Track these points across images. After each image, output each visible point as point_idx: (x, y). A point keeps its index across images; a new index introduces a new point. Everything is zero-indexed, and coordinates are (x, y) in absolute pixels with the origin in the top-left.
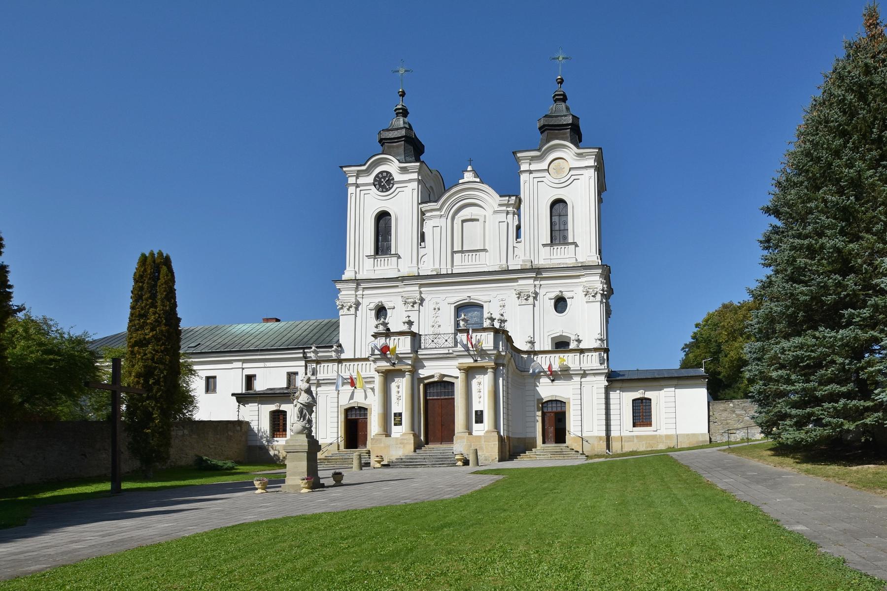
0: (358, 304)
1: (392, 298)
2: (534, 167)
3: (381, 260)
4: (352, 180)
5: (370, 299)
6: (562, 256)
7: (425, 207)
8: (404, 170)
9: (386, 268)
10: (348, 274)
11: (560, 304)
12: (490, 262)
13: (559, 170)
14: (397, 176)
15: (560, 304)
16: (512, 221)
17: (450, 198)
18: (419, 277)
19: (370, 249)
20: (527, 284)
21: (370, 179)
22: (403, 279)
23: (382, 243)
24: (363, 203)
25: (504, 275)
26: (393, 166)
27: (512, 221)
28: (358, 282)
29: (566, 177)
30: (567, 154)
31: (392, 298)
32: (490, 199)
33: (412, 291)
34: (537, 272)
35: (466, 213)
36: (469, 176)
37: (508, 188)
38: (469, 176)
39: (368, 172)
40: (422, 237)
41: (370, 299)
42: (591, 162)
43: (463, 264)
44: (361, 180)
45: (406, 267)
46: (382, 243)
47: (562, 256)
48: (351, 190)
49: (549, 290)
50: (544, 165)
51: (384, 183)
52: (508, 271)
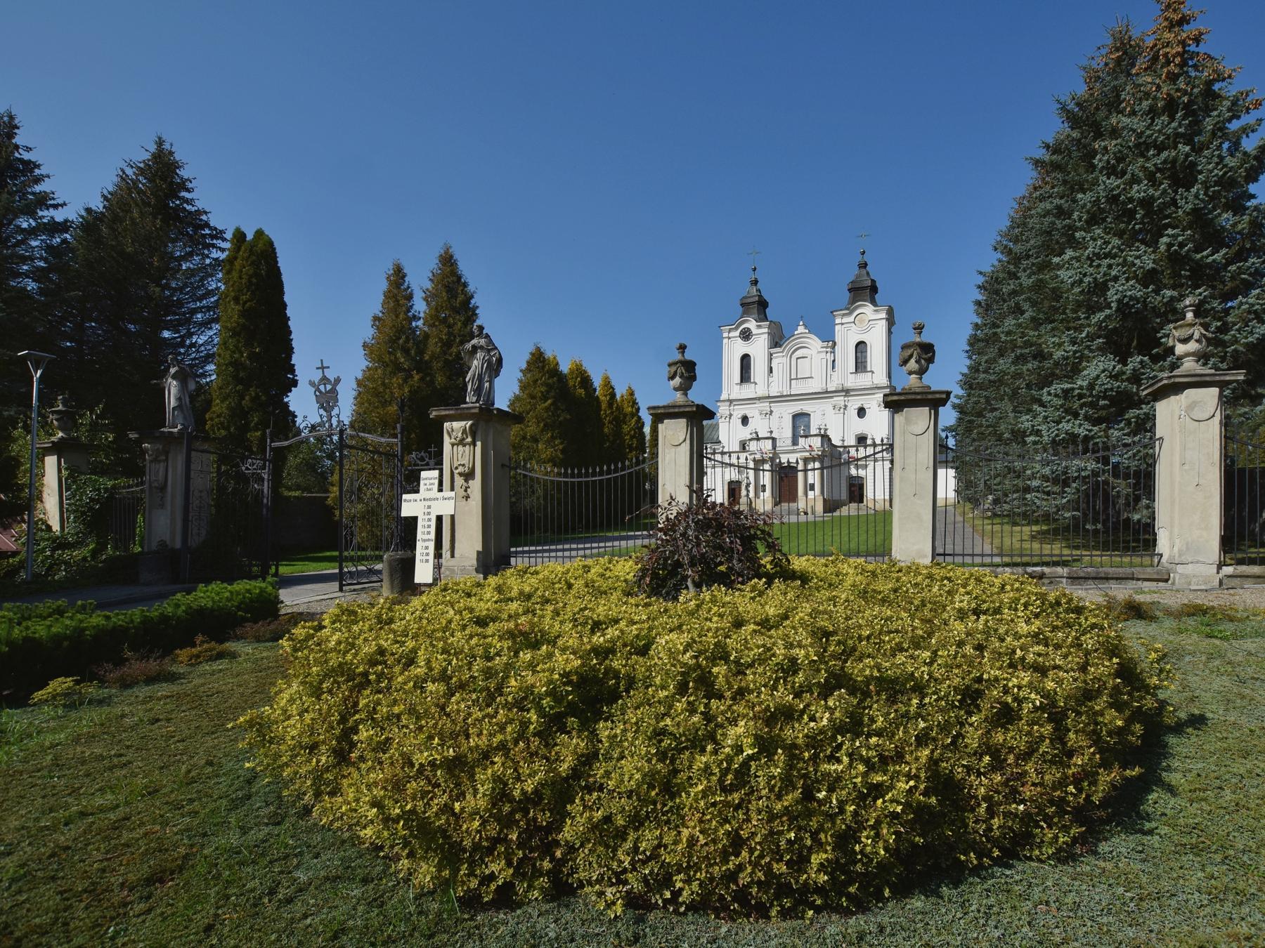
0: (731, 415)
1: (752, 411)
2: (845, 320)
3: (745, 385)
4: (725, 335)
5: (739, 412)
6: (863, 380)
7: (773, 351)
8: (759, 327)
9: (748, 391)
10: (724, 396)
11: (861, 412)
12: (815, 386)
13: (861, 321)
14: (755, 331)
15: (861, 412)
16: (830, 357)
17: (789, 345)
18: (769, 397)
19: (737, 378)
20: (839, 400)
21: (737, 333)
22: (759, 399)
23: (745, 376)
24: (733, 349)
25: (825, 394)
26: (752, 324)
27: (830, 357)
28: (731, 401)
29: (867, 326)
30: (867, 310)
31: (752, 411)
32: (815, 343)
33: (765, 406)
34: (847, 392)
35: (799, 353)
36: (801, 329)
37: (829, 340)
38: (801, 329)
39: (736, 328)
40: (771, 370)
41: (739, 412)
42: (884, 315)
43: (798, 388)
44: (732, 334)
45: (761, 391)
46: (745, 376)
47: (863, 380)
48: (725, 341)
49: (854, 403)
50: (851, 319)
51: (746, 335)
52: (827, 392)
